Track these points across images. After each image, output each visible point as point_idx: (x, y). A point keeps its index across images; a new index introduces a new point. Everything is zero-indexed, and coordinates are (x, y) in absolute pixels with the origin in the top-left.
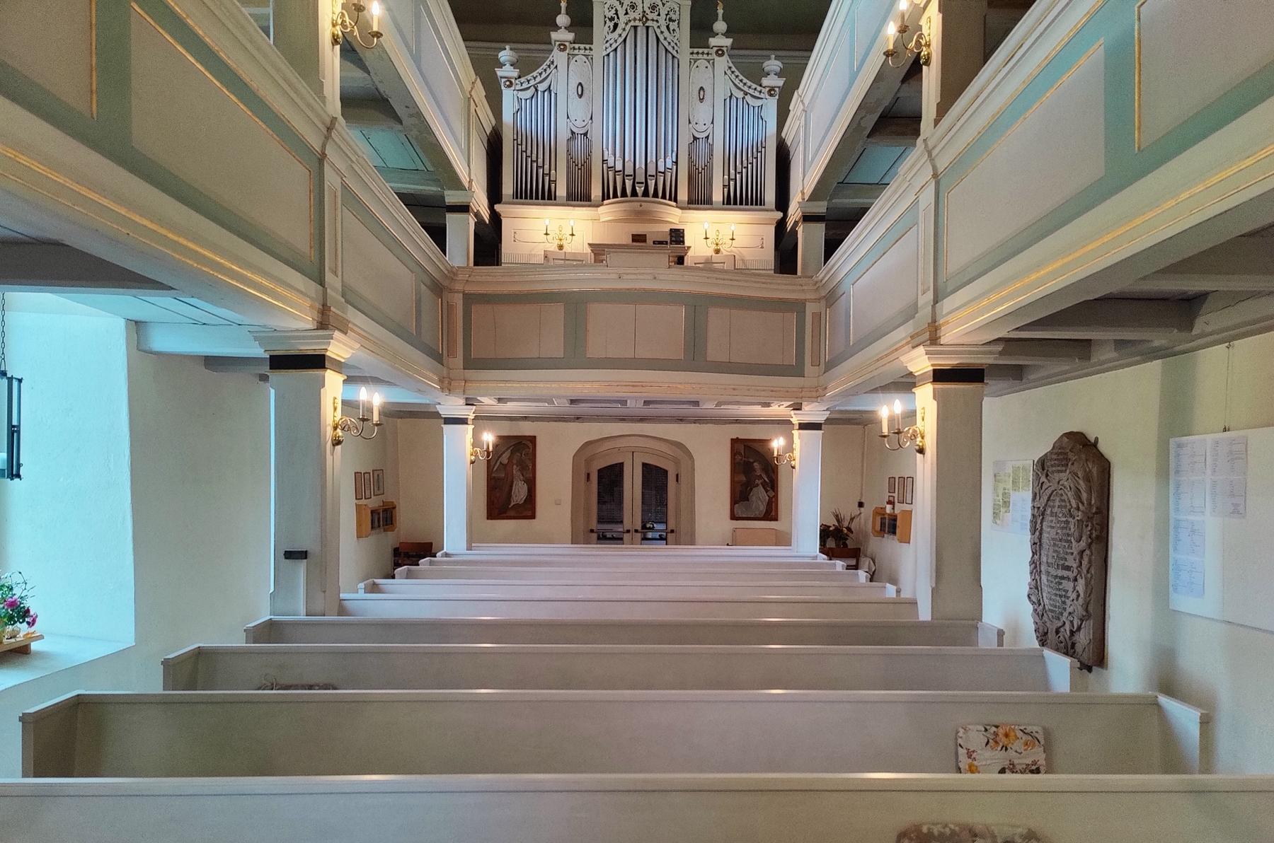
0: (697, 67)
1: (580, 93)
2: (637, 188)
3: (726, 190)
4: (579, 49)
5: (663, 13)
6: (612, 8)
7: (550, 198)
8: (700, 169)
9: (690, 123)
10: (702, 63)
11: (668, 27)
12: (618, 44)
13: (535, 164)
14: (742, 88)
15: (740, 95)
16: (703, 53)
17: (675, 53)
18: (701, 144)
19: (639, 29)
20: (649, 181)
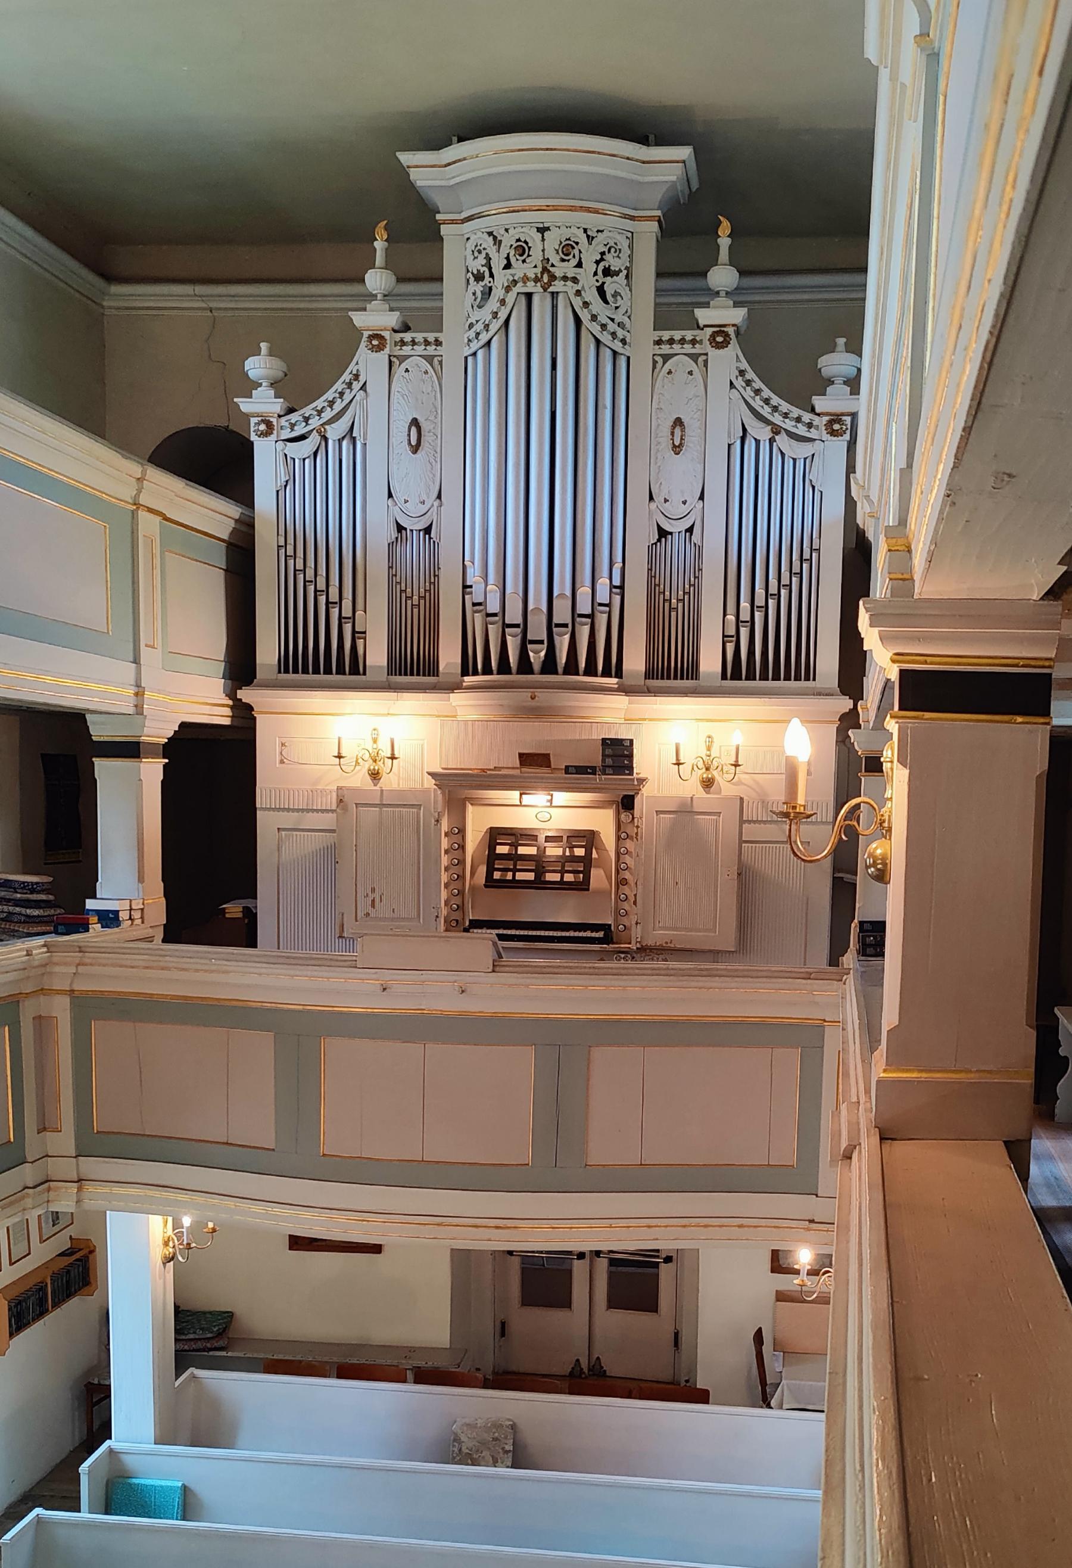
0: (670, 372)
1: (414, 442)
2: (531, 654)
4: (414, 343)
5: (589, 256)
6: (480, 252)
7: (355, 671)
8: (674, 601)
9: (651, 498)
10: (681, 363)
11: (601, 291)
12: (491, 333)
13: (322, 599)
14: (770, 417)
15: (763, 433)
16: (682, 341)
17: (617, 346)
18: (676, 542)
19: (536, 300)
20: (556, 637)
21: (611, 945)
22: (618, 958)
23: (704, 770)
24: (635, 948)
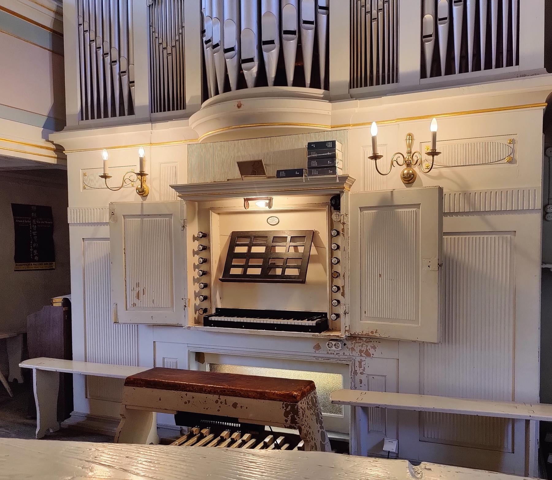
3: (429, 46)
21: (323, 334)
22: (330, 345)
23: (405, 166)
24: (344, 336)
